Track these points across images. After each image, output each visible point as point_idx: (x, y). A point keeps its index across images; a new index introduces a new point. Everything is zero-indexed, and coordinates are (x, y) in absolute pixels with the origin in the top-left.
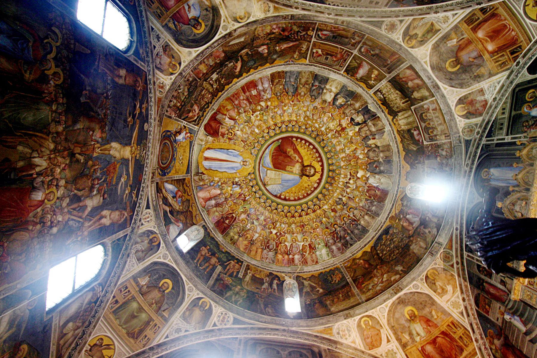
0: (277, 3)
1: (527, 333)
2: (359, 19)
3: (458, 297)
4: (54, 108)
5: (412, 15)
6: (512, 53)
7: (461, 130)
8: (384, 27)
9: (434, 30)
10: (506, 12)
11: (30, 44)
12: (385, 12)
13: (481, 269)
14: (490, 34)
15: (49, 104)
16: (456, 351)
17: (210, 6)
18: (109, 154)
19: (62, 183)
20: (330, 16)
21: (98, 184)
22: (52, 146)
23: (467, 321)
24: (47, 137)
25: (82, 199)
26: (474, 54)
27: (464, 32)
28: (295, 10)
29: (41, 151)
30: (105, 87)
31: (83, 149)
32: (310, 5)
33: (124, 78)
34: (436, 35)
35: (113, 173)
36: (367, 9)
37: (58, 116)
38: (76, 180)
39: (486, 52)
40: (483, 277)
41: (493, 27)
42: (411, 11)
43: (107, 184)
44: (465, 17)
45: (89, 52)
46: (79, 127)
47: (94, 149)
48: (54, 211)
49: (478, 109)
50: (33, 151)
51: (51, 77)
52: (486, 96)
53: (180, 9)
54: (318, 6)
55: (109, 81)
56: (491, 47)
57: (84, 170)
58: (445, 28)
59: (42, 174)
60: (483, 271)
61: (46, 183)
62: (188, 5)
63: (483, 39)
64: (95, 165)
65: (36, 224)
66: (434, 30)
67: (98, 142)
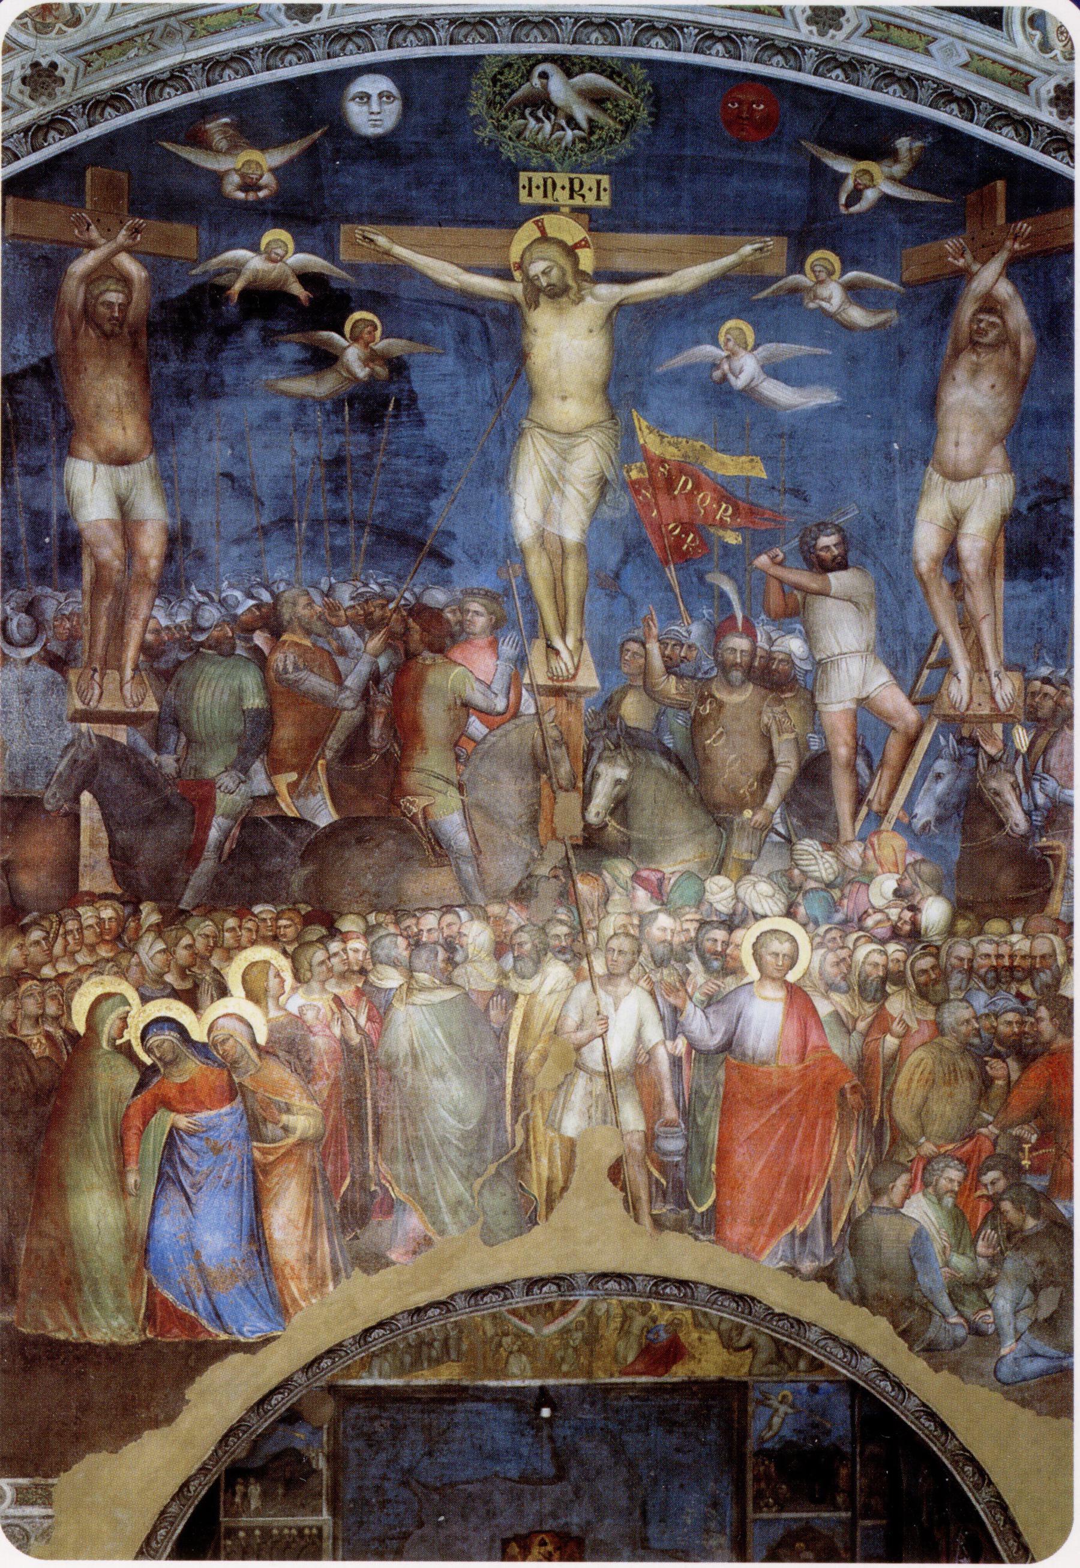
4: (391, 979)
11: (182, 1121)
15: (380, 1015)
18: (582, 548)
19: (720, 892)
21: (749, 631)
22: (556, 972)
24: (521, 1000)
25: (815, 746)
29: (580, 1027)
30: (223, 649)
31: (564, 770)
33: (124, 475)
35: (698, 487)
37: (424, 954)
38: (718, 807)
43: (760, 542)
45: (86, 797)
46: (457, 818)
47: (558, 692)
48: (846, 922)
50: (579, 1066)
51: (274, 1013)
55: (182, 618)
57: (666, 753)
59: (676, 1010)
61: (712, 987)
64: (646, 671)
65: (881, 1022)
67: (521, 661)
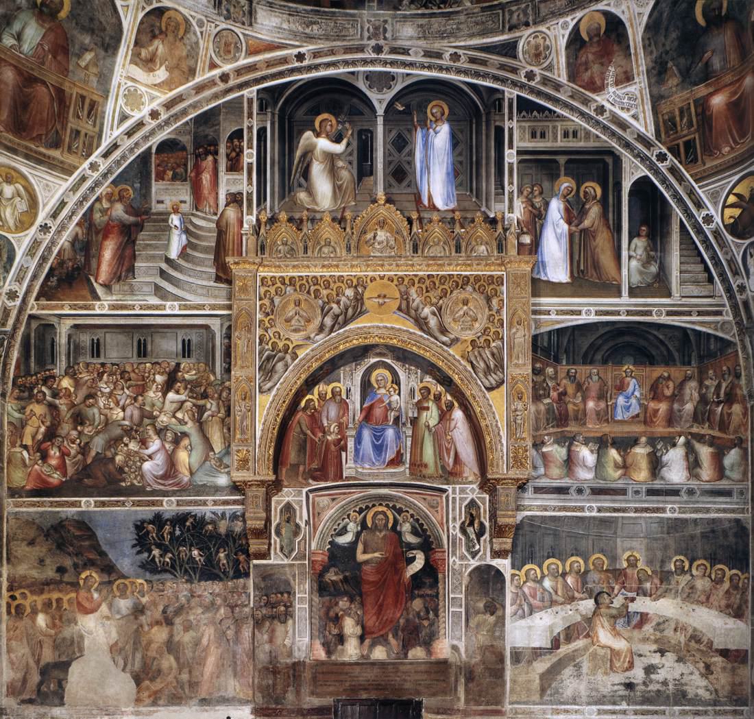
1: (168, 261)
3: (153, 99)
6: (689, 145)
7: (543, 28)
13: (236, 142)
16: (47, 135)
23: (116, 133)
40: (223, 150)
49: (586, 70)
52: (611, 89)
60: (234, 150)
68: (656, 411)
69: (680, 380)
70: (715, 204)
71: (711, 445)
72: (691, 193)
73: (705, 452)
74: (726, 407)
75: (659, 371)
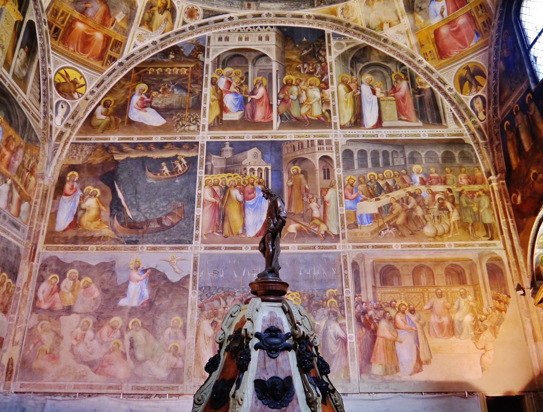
0: (333, 21)
2: (232, 15)
5: (177, 33)
6: (57, 30)
8: (201, 12)
9: (145, 24)
10: (93, 65)
12: (207, 30)
14: (90, 39)
17: (415, 13)
20: (266, 12)
26: (90, 12)
27: (115, 32)
28: (311, 14)
32: (293, 23)
34: (141, 19)
36: (227, 29)
39: (81, 19)
41: (93, 47)
42: (180, 38)
44: (124, 47)
53: (454, 11)
54: (284, 22)
56: (80, 26)
58: (136, 30)
62: (442, 16)
63: (92, 31)
66: (145, 24)
68: (5, 155)
69: (18, 145)
70: (55, 67)
71: (19, 193)
72: (48, 51)
73: (16, 196)
74: (29, 176)
75: (11, 132)
